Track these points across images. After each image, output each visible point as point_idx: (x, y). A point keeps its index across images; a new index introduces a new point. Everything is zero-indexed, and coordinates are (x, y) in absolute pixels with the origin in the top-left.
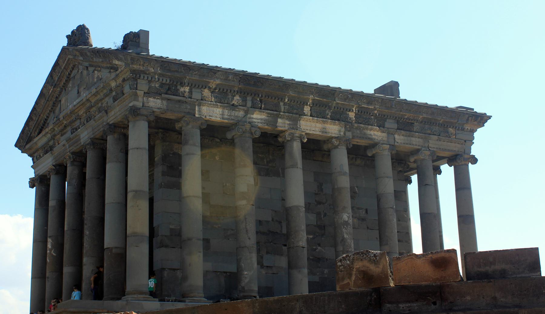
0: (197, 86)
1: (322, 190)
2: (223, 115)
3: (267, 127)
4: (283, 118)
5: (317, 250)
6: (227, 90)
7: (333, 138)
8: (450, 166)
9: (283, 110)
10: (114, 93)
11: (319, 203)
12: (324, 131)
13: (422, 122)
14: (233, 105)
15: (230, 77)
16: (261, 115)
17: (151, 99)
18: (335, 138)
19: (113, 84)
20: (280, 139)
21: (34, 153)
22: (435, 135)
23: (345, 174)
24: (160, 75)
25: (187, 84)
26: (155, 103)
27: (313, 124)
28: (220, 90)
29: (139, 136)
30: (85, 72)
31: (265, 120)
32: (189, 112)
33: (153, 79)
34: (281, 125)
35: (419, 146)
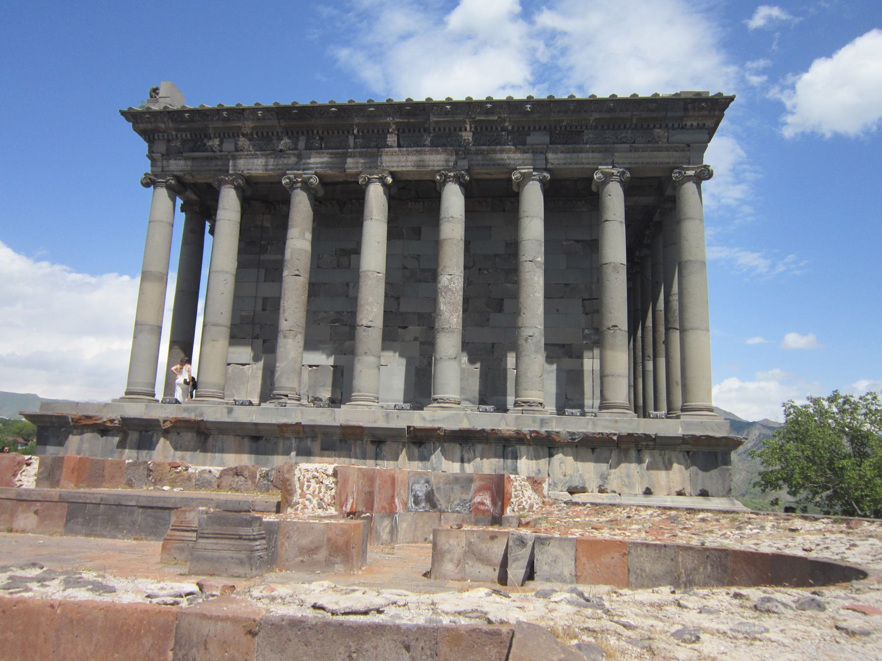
2: (266, 165)
3: (329, 172)
4: (355, 156)
6: (268, 133)
12: (420, 164)
14: (281, 151)
15: (260, 113)
17: (172, 162)
18: (439, 171)
22: (625, 143)
26: (177, 165)
27: (404, 158)
28: (257, 134)
31: (327, 163)
32: (220, 170)
34: (351, 166)
35: (593, 164)
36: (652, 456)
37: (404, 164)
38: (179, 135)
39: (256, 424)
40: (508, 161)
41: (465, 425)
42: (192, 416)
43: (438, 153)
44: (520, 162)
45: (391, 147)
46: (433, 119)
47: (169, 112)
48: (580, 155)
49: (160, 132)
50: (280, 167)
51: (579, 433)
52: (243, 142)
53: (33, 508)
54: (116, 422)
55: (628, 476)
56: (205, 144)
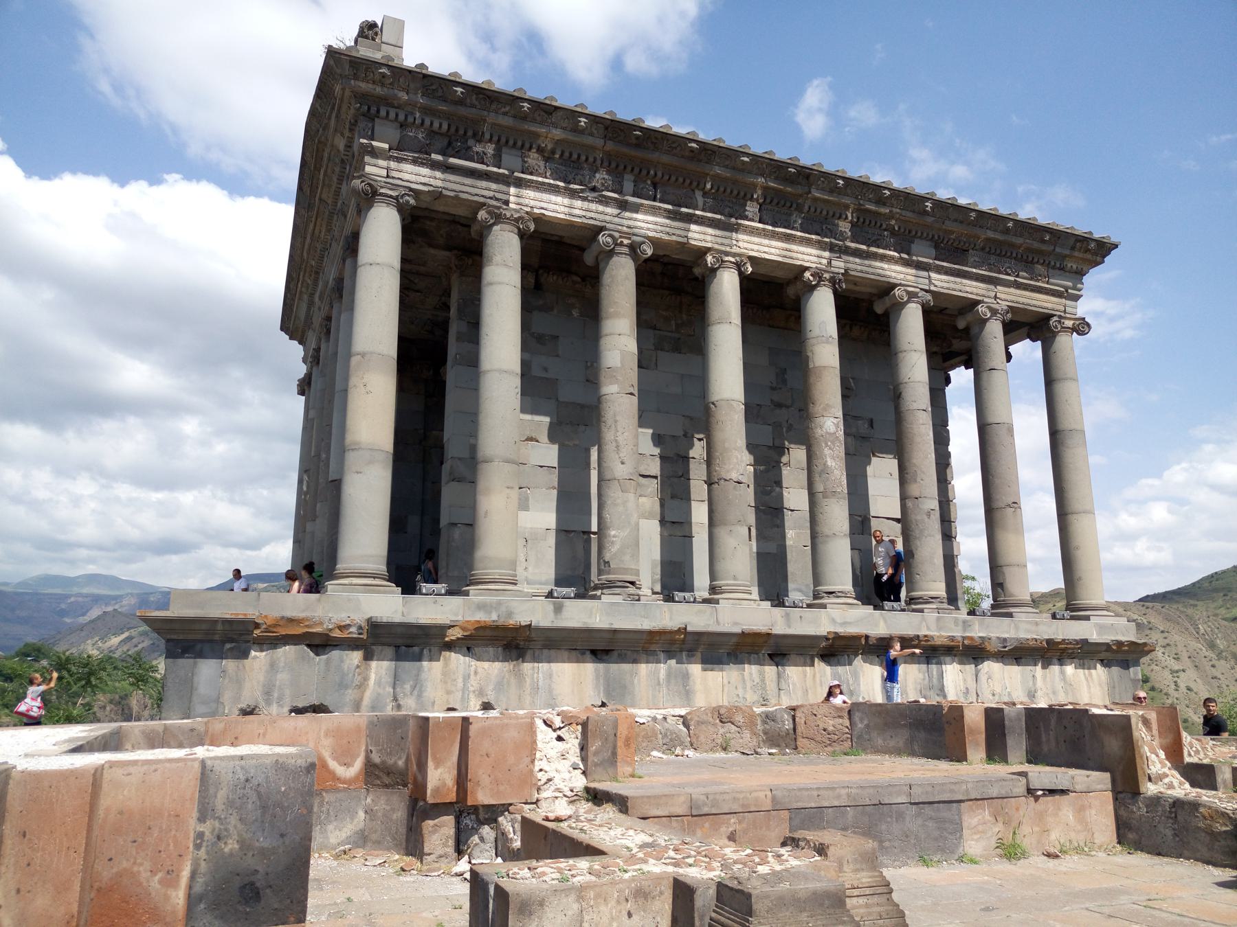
0: (511, 142)
1: (784, 381)
3: (666, 237)
5: (773, 494)
7: (807, 268)
8: (1034, 340)
9: (700, 203)
11: (779, 405)
13: (983, 249)
16: (654, 214)
20: (697, 271)
21: (302, 336)
23: (828, 340)
24: (426, 111)
25: (487, 136)
26: (416, 176)
27: (766, 242)
33: (410, 120)
34: (696, 236)
37: (766, 249)
38: (427, 122)
39: (615, 631)
40: (888, 273)
42: (492, 617)
43: (808, 243)
44: (902, 276)
45: (752, 220)
47: (425, 76)
49: (394, 107)
50: (593, 215)
51: (1011, 639)
52: (534, 159)
53: (725, 830)
54: (353, 629)
55: (1054, 693)
56: (470, 148)
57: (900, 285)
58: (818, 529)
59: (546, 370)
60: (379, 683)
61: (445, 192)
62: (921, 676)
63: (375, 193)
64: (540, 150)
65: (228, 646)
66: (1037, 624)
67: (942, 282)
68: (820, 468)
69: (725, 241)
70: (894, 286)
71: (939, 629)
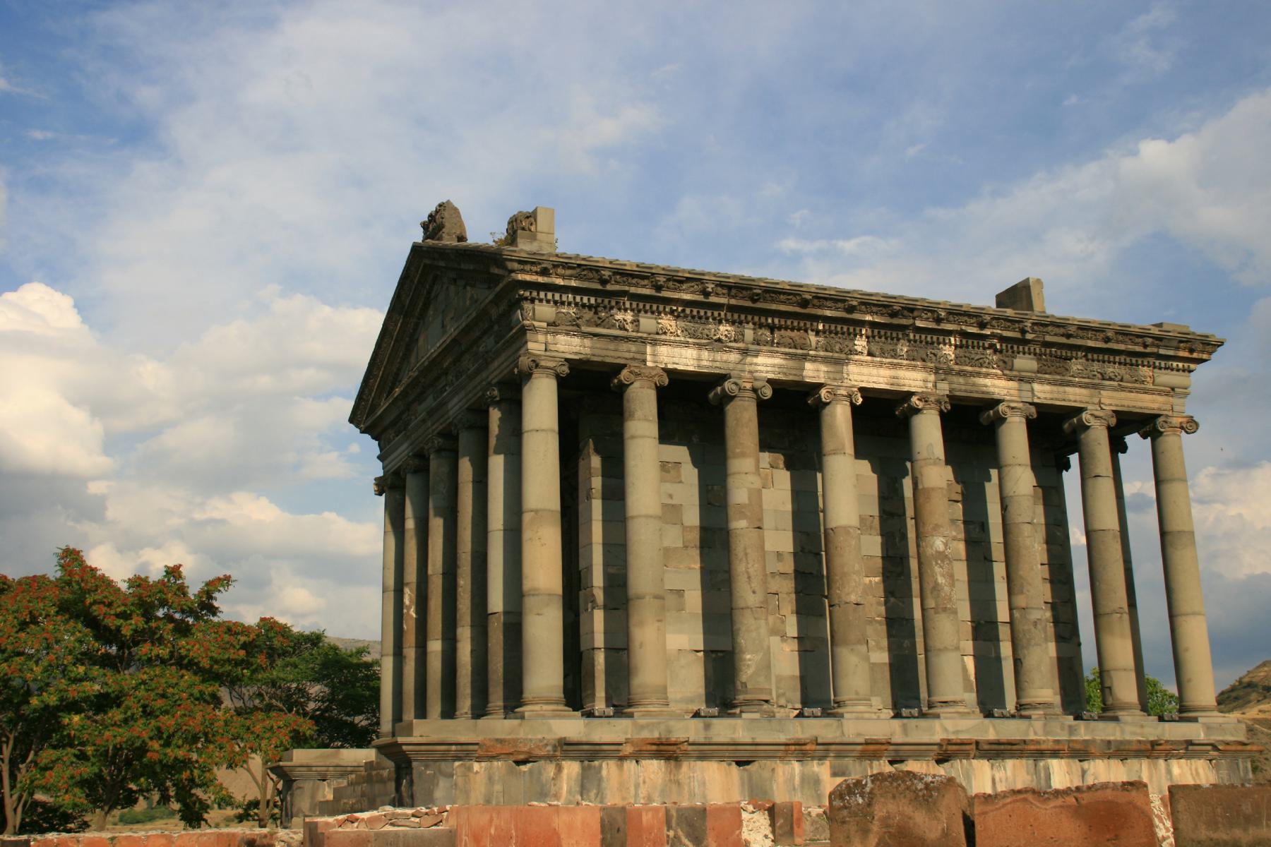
2: (699, 359)
4: (815, 361)
7: (913, 394)
8: (1144, 437)
9: (814, 344)
10: (496, 327)
14: (719, 340)
19: (494, 313)
23: (936, 462)
25: (628, 305)
26: (570, 346)
27: (874, 371)
29: (541, 405)
30: (452, 288)
31: (780, 366)
34: (811, 374)
36: (1180, 767)
37: (875, 379)
40: (992, 389)
41: (992, 736)
44: (1005, 392)
46: (919, 324)
48: (1067, 389)
50: (718, 364)
52: (667, 322)
57: (1003, 401)
58: (930, 643)
59: (671, 496)
60: (570, 791)
61: (595, 359)
62: (1029, 777)
63: (537, 366)
64: (672, 312)
65: (457, 764)
66: (1142, 726)
67: (1044, 392)
68: (931, 585)
69: (838, 376)
70: (998, 402)
71: (1046, 733)
